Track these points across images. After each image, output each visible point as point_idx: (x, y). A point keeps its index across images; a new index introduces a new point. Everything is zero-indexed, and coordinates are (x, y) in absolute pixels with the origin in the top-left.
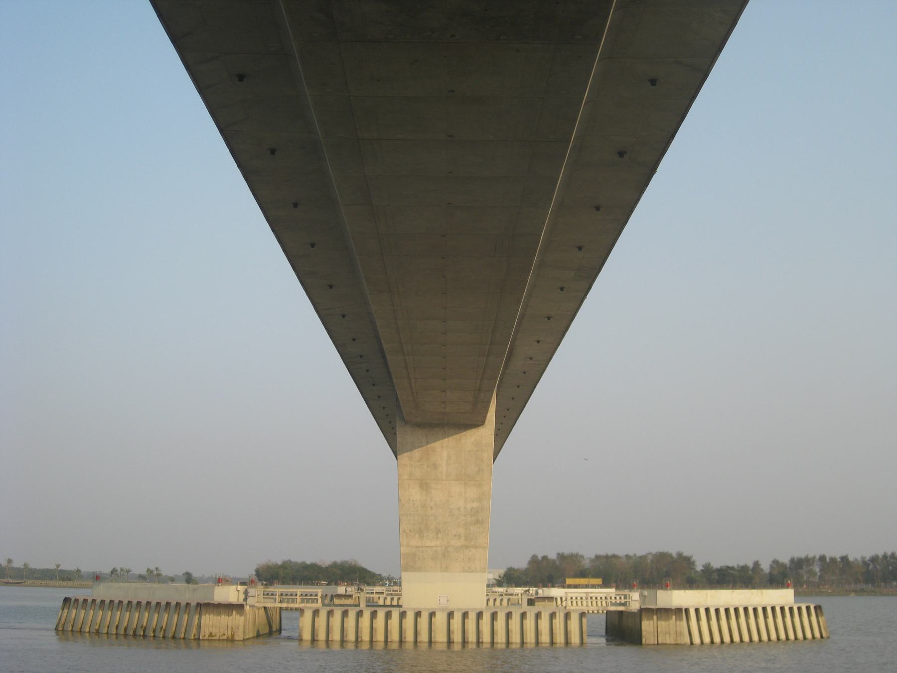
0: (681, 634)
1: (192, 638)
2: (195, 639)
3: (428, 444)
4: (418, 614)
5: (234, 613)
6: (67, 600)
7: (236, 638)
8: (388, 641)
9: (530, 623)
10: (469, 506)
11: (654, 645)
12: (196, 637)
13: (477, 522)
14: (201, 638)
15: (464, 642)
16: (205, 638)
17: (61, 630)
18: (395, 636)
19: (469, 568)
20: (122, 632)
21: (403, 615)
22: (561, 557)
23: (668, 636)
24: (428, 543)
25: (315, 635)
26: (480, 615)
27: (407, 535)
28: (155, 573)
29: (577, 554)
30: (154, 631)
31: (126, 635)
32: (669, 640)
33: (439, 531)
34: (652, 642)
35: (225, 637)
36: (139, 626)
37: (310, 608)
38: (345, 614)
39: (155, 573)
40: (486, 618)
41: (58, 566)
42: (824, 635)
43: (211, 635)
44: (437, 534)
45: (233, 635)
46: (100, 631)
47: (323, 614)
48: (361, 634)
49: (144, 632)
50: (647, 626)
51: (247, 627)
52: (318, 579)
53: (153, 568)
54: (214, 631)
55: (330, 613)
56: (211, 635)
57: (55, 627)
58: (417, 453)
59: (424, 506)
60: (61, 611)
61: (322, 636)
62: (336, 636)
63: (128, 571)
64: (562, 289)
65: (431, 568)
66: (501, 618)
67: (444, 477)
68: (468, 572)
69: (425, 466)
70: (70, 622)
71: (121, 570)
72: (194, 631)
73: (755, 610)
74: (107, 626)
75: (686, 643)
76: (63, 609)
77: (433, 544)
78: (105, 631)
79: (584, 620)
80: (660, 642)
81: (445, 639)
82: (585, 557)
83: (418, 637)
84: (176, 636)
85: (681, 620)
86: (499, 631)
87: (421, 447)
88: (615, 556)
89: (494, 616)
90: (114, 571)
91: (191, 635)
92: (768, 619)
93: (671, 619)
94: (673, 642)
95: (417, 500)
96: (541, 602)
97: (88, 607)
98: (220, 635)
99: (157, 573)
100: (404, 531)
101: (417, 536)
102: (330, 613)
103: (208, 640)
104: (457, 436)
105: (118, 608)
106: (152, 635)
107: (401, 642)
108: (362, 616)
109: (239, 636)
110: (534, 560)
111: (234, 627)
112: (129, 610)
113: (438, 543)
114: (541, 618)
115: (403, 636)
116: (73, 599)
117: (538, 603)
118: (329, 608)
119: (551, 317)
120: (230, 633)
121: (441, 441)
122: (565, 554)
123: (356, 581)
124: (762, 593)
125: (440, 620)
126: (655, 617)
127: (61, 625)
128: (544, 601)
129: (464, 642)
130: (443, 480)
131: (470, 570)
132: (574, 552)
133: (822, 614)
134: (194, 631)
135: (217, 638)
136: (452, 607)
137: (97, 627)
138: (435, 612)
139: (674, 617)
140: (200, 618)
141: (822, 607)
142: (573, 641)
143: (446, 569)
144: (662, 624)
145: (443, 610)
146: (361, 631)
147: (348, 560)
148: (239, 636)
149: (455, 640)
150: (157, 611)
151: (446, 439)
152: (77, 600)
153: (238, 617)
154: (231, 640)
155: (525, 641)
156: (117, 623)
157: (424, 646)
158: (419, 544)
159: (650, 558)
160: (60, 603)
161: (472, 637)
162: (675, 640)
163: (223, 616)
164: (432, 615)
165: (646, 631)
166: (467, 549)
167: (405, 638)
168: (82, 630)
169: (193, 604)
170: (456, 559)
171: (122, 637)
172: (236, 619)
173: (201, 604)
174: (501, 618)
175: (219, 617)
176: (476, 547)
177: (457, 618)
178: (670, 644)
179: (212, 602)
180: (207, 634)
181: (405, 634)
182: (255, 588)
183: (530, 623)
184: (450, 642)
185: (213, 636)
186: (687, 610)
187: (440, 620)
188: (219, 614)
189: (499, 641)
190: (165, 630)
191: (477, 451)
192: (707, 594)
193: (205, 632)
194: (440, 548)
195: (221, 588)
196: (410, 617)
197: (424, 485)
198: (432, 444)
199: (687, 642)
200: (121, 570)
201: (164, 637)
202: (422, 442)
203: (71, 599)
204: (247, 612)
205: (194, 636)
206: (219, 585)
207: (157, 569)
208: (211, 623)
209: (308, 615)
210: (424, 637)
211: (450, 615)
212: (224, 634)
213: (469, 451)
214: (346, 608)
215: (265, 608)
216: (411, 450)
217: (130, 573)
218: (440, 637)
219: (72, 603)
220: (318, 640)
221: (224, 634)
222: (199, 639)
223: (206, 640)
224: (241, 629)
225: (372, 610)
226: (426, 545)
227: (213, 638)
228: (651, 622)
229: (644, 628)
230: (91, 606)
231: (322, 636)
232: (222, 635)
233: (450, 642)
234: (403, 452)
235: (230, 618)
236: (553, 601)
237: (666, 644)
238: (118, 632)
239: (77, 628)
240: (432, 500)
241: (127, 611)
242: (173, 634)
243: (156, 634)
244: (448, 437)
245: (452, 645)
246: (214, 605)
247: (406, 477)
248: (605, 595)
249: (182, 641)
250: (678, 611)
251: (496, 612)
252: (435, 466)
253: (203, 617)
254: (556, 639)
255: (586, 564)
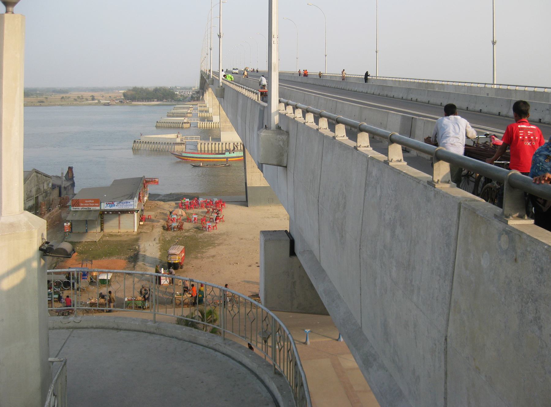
30: (162, 149)
36: (157, 148)
43: (177, 150)
52: (153, 98)
56: (177, 150)
84: (168, 150)
137: (145, 148)
140: (174, 146)
164: (229, 144)
169: (172, 143)
196: (224, 144)
222: (174, 151)
246: (178, 143)
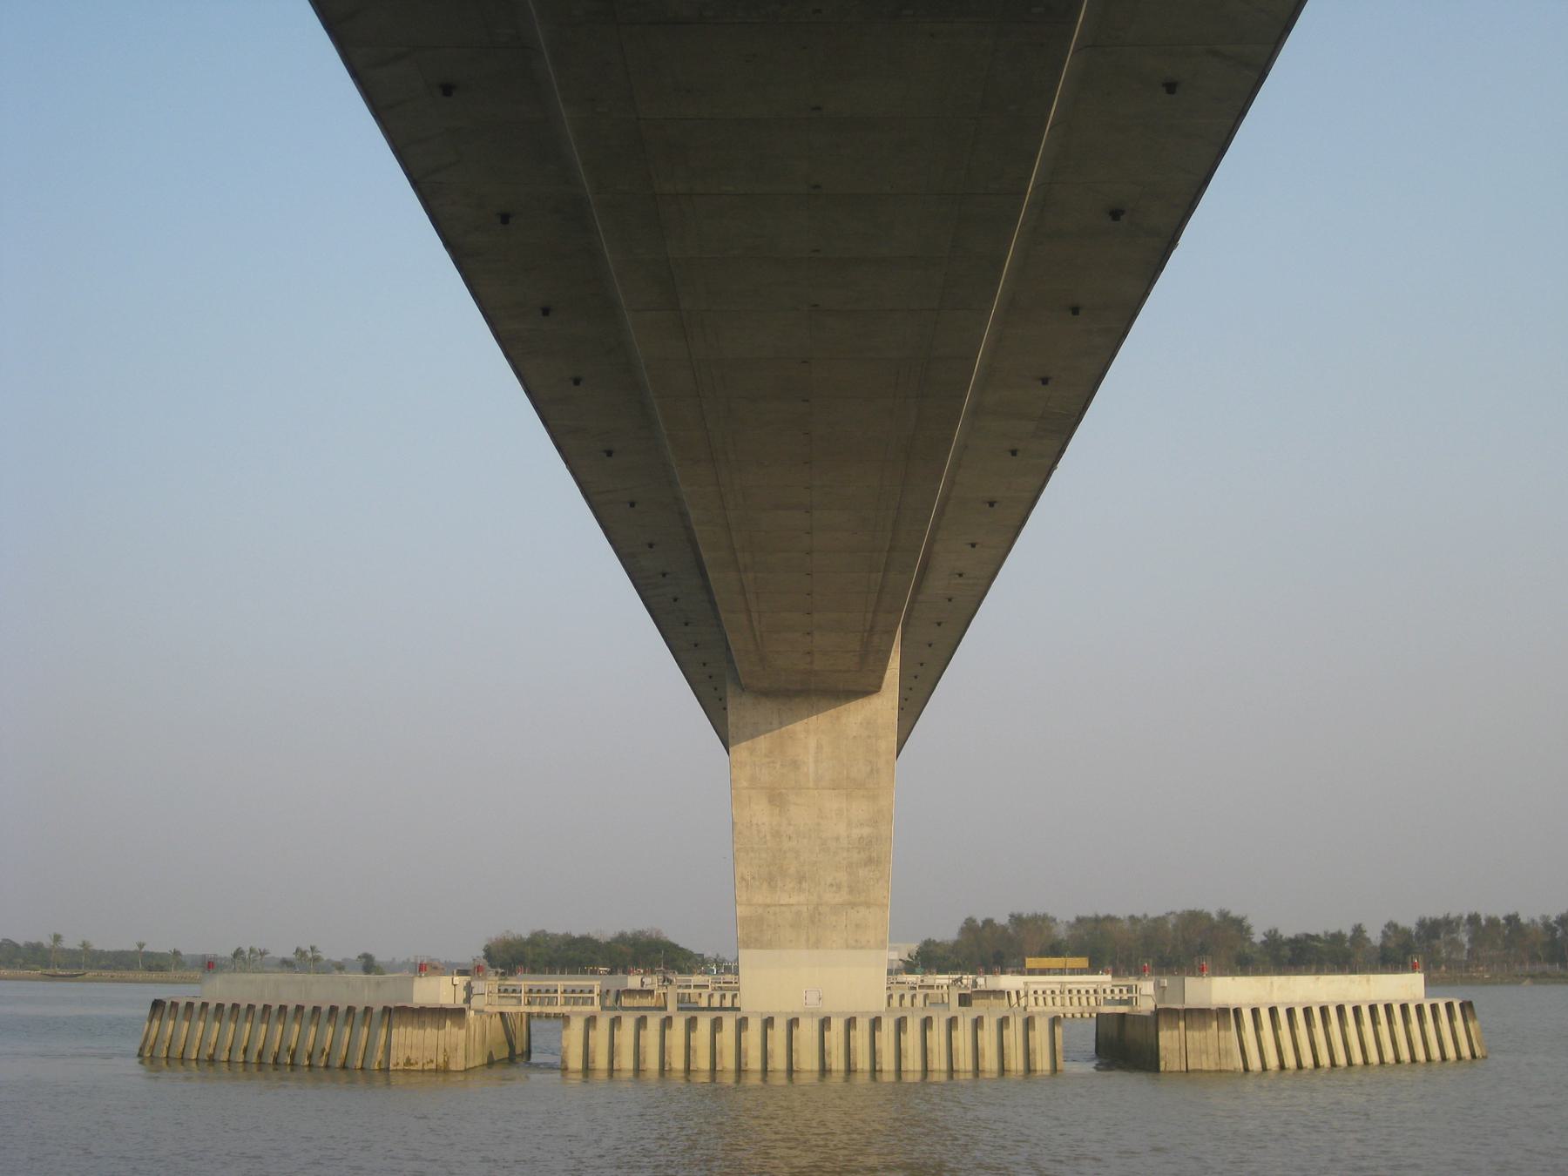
0: (1228, 1052)
1: (376, 1067)
2: (380, 1070)
3: (782, 727)
4: (768, 1023)
5: (448, 1023)
6: (157, 1005)
7: (453, 1067)
8: (717, 1069)
9: (963, 1037)
10: (856, 833)
11: (1181, 1072)
12: (383, 1066)
13: (870, 861)
14: (391, 1067)
15: (850, 1070)
16: (398, 1068)
17: (148, 1056)
18: (728, 1061)
19: (856, 941)
20: (254, 1059)
21: (742, 1024)
22: (1017, 920)
23: (1204, 1057)
24: (785, 900)
25: (590, 1060)
26: (875, 1023)
27: (747, 886)
28: (310, 955)
29: (1044, 915)
30: (310, 1057)
31: (261, 1064)
32: (1208, 1063)
33: (804, 877)
34: (1176, 1068)
35: (433, 1066)
36: (284, 1048)
37: (580, 1014)
38: (641, 1023)
39: (310, 955)
40: (888, 1026)
41: (141, 946)
42: (1478, 1053)
43: (408, 1062)
44: (800, 883)
45: (446, 1063)
46: (216, 1057)
47: (603, 1024)
48: (670, 1057)
49: (293, 1058)
50: (1168, 1039)
51: (471, 1048)
52: (592, 962)
53: (306, 947)
54: (414, 1055)
55: (615, 1023)
56: (408, 1062)
57: (137, 1051)
58: (762, 742)
59: (777, 834)
60: (147, 1024)
61: (601, 1061)
62: (626, 1061)
63: (263, 954)
64: (1014, 453)
65: (791, 941)
66: (913, 1027)
67: (811, 785)
68: (854, 948)
69: (778, 766)
70: (164, 1042)
71: (252, 950)
72: (379, 1055)
73: (1357, 1010)
74: (228, 1048)
75: (1235, 1069)
76: (151, 1021)
77: (793, 900)
78: (224, 1056)
79: (1059, 1031)
80: (1190, 1068)
81: (816, 1066)
82: (1058, 920)
83: (769, 1061)
84: (349, 1064)
85: (1228, 1028)
86: (910, 1051)
87: (771, 731)
88: (1110, 919)
89: (900, 1025)
90: (238, 953)
91: (375, 1063)
92: (1379, 1027)
93: (1211, 1026)
94: (1213, 1067)
95: (763, 824)
96: (982, 998)
97: (195, 1016)
98: (425, 1061)
99: (313, 957)
100: (743, 879)
101: (765, 885)
102: (615, 1023)
103: (404, 1070)
104: (832, 712)
105: (247, 1017)
106: (307, 1063)
107: (740, 1070)
108: (670, 1026)
109: (458, 1063)
110: (969, 927)
111: (448, 1050)
112: (266, 1019)
113: (802, 898)
114: (982, 1028)
115: (743, 1060)
116: (168, 1004)
117: (977, 1001)
118: (613, 1014)
119: (995, 502)
120: (441, 1060)
121: (805, 721)
122: (1025, 916)
123: (660, 966)
124: (1368, 981)
125: (807, 1032)
126: (1182, 1024)
127: (147, 1049)
128: (988, 998)
129: (850, 1070)
130: (808, 788)
131: (858, 946)
132: (1040, 912)
133: (1474, 1017)
134: (379, 1055)
135: (419, 1067)
136: (826, 1009)
138: (797, 1019)
139: (1215, 1024)
141: (1474, 1005)
142: (1039, 1067)
143: (817, 945)
144: (1195, 1036)
145: (812, 1015)
146: (670, 1053)
147: (645, 930)
148: (458, 1063)
149: (834, 1067)
150: (315, 1021)
151: (814, 717)
152: (174, 1005)
153: (455, 1030)
154: (444, 1071)
155: (955, 1067)
156: (245, 1044)
157: (780, 1079)
158: (768, 901)
159: (1172, 920)
160: (147, 1011)
161: (862, 1062)
162: (1217, 1064)
163: (428, 1030)
164: (793, 1023)
165: (1166, 1048)
166: (852, 908)
167: (746, 1064)
168: (185, 1056)
169: (378, 1008)
170: (835, 926)
171: (254, 1069)
172: (451, 1033)
173: (391, 1009)
174: (913, 1027)
175: (421, 1032)
176: (868, 905)
177: (837, 1026)
178: (1209, 1072)
179: (409, 1006)
180: (402, 1061)
181: (746, 1056)
182: (482, 980)
183: (963, 1037)
184: (824, 1070)
185: (412, 1064)
186: (1237, 1012)
187: (807, 1032)
188: (423, 1026)
189: (910, 1067)
190: (328, 1055)
191: (869, 737)
192: (1272, 983)
193: (398, 1057)
194: (805, 909)
195: (424, 980)
196: (755, 1027)
197: (776, 798)
198: (790, 727)
199: (1237, 1066)
200: (252, 950)
201: (327, 1066)
202: (771, 724)
203: (165, 1003)
204: (471, 1022)
205: (380, 1063)
206: (421, 976)
207: (312, 949)
208: (410, 1042)
209: (577, 1026)
210: (779, 1062)
211: (825, 1023)
212: (432, 1061)
213: (855, 737)
214: (643, 1013)
215: (502, 1014)
216: (752, 737)
217: (266, 956)
218: (808, 1060)
219: (167, 1010)
220: (594, 1070)
221: (432, 1061)
222: (388, 1069)
223: (400, 1070)
224: (461, 1052)
225: (689, 1017)
226: (782, 902)
227: (412, 1068)
228: (1176, 1033)
229: (1162, 1043)
230: (200, 1015)
231: (601, 1061)
232: (428, 1063)
233: (824, 1070)
234: (739, 742)
235: (441, 1032)
236: (1003, 998)
237: (1201, 1071)
238: (247, 1059)
239: (176, 1052)
240: (790, 824)
241: (262, 1023)
242: (343, 1060)
243: (314, 1062)
244: (817, 714)
245: (827, 1075)
246: (413, 1010)
247: (745, 784)
248: (1095, 986)
249: (359, 1072)
250: (1223, 1012)
251: (905, 1018)
252: (795, 765)
253: (394, 1031)
254: (1009, 1062)
255: (1061, 932)
